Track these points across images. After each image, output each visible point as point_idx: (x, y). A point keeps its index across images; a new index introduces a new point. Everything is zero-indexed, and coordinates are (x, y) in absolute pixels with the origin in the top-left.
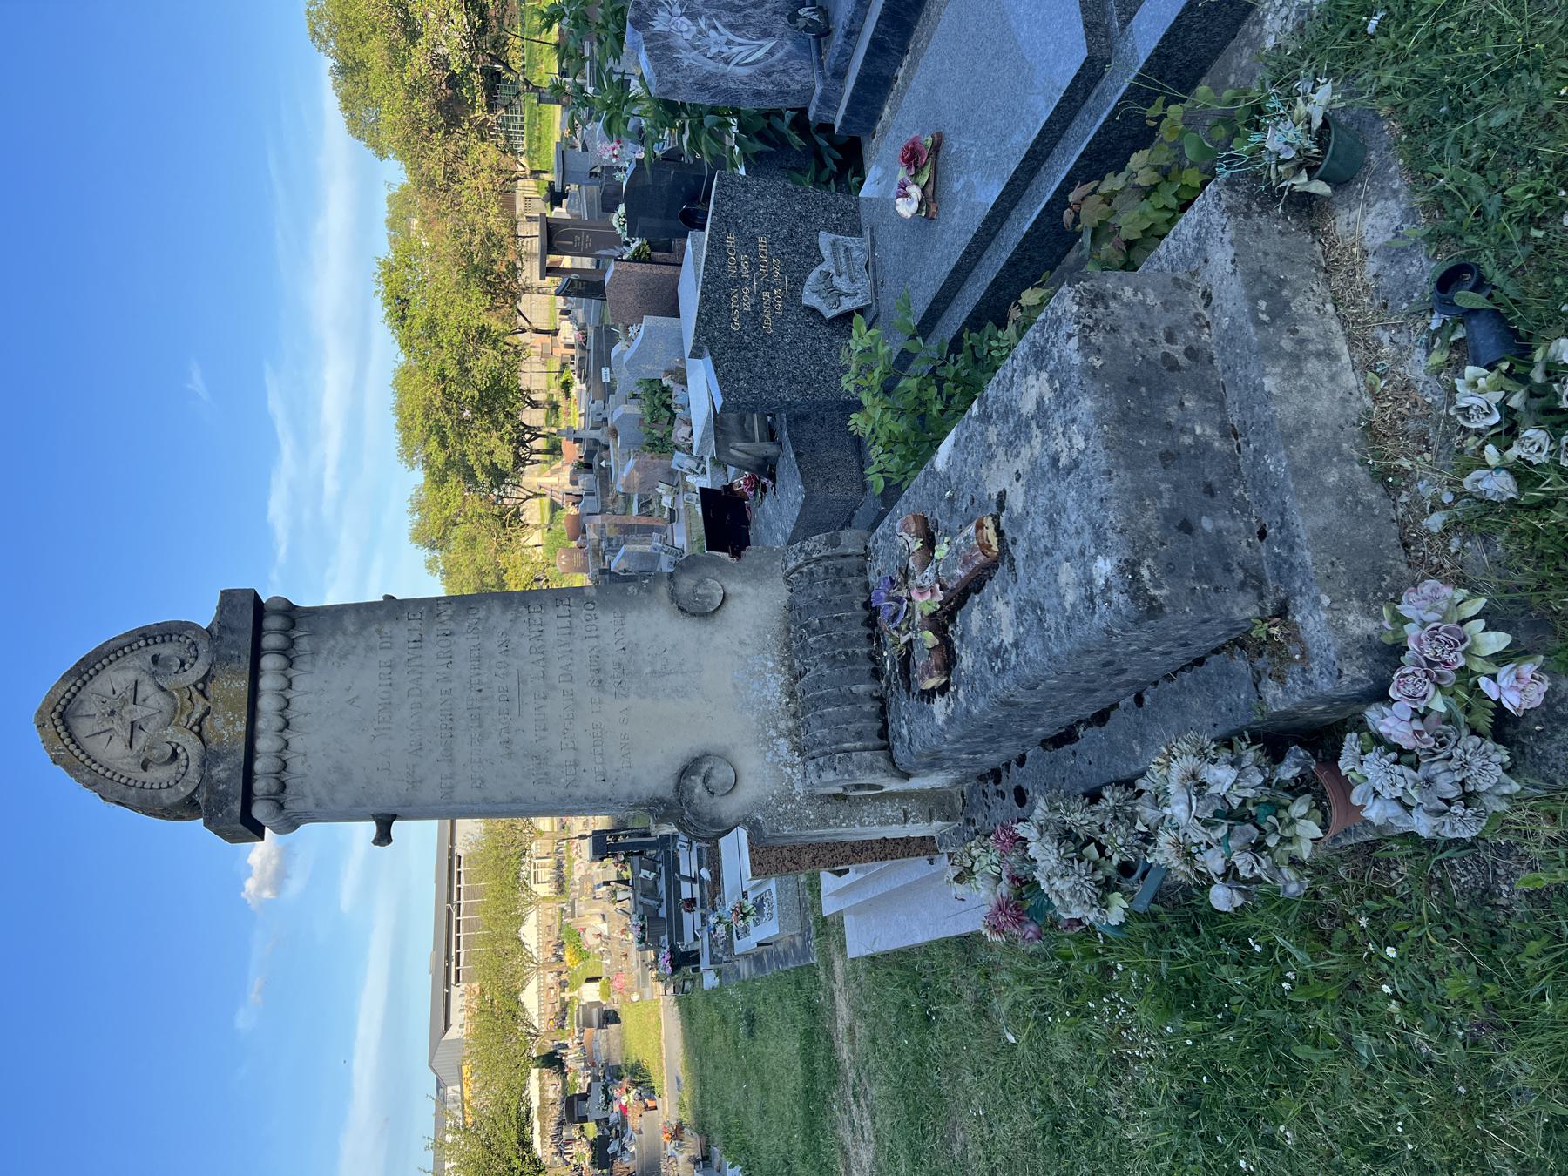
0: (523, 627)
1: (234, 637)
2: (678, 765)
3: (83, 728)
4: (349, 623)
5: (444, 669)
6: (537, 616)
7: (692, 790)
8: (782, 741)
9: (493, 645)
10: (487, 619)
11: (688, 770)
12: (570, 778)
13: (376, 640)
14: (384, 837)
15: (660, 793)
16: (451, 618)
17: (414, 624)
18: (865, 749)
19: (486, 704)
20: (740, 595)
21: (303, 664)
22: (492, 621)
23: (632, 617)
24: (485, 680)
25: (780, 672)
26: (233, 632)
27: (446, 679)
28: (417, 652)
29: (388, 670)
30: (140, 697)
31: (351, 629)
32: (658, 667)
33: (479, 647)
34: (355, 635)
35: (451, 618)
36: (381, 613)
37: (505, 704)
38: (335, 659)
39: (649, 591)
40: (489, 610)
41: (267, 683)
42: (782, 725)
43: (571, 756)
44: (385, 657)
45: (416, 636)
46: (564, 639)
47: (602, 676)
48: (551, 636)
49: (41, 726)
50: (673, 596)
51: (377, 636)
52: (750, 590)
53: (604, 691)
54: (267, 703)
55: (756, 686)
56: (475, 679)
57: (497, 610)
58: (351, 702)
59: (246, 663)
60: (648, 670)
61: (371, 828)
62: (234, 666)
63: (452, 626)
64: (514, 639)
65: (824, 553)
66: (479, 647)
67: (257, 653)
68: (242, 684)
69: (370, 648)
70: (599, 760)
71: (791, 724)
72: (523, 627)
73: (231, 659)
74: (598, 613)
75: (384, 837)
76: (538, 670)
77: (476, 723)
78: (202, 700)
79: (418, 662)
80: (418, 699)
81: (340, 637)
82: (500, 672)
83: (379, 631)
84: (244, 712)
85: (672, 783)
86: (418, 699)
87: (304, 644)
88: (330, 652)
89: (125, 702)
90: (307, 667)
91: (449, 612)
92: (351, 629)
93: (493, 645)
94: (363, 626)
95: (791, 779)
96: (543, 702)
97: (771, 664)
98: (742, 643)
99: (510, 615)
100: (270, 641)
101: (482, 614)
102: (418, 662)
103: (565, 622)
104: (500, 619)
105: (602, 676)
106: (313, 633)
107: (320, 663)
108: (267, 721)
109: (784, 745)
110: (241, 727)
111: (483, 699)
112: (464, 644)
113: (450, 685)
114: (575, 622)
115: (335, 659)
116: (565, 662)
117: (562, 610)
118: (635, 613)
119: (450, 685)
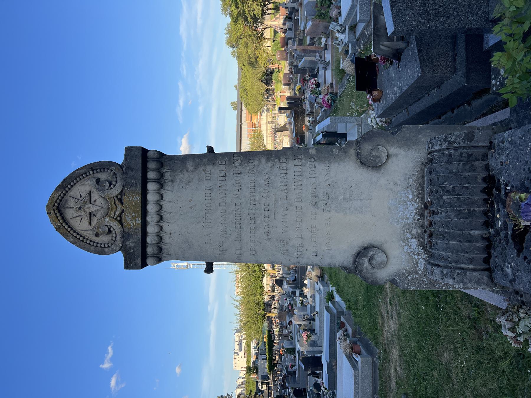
0: (276, 171)
1: (133, 173)
2: (355, 251)
3: (69, 214)
4: (190, 165)
5: (237, 193)
6: (284, 165)
7: (362, 265)
8: (414, 240)
9: (261, 180)
10: (258, 166)
11: (362, 252)
12: (299, 253)
13: (203, 175)
14: (209, 269)
15: (345, 264)
17: (222, 167)
18: (475, 270)
19: (258, 212)
20: (396, 155)
21: (168, 186)
22: (261, 166)
23: (335, 167)
24: (257, 199)
25: (416, 201)
26: (132, 170)
27: (238, 198)
28: (223, 183)
29: (210, 192)
30: (93, 200)
31: (191, 168)
32: (347, 196)
33: (254, 181)
34: (193, 172)
36: (205, 160)
37: (267, 213)
39: (345, 152)
40: (260, 161)
41: (151, 197)
42: (414, 231)
44: (208, 184)
45: (223, 174)
47: (317, 199)
49: (49, 213)
50: (358, 154)
51: (203, 173)
52: (402, 152)
53: (318, 208)
54: (151, 208)
55: (401, 209)
56: (252, 198)
57: (263, 161)
58: (192, 208)
59: (139, 187)
60: (342, 197)
61: (203, 265)
62: (134, 188)
63: (240, 169)
64: (272, 177)
65: (462, 144)
66: (254, 181)
67: (145, 181)
68: (138, 199)
69: (200, 179)
70: (314, 244)
71: (419, 231)
72: (276, 171)
73: (132, 185)
74: (316, 164)
75: (209, 269)
76: (284, 195)
77: (253, 222)
78: (120, 206)
79: (224, 188)
80: (225, 208)
82: (265, 195)
83: (204, 170)
84: (140, 213)
85: (351, 259)
86: (225, 208)
87: (168, 176)
89: (85, 202)
90: (169, 188)
91: (239, 161)
92: (191, 168)
93: (261, 180)
94: (197, 167)
95: (417, 262)
96: (286, 212)
97: (411, 197)
98: (395, 184)
99: (270, 164)
100: (151, 175)
101: (256, 163)
102: (224, 188)
103: (298, 169)
104: (265, 166)
105: (317, 199)
106: (172, 170)
107: (176, 187)
108: (152, 218)
109: (414, 243)
110: (139, 221)
111: (256, 209)
112: (246, 178)
114: (304, 168)
116: (298, 191)
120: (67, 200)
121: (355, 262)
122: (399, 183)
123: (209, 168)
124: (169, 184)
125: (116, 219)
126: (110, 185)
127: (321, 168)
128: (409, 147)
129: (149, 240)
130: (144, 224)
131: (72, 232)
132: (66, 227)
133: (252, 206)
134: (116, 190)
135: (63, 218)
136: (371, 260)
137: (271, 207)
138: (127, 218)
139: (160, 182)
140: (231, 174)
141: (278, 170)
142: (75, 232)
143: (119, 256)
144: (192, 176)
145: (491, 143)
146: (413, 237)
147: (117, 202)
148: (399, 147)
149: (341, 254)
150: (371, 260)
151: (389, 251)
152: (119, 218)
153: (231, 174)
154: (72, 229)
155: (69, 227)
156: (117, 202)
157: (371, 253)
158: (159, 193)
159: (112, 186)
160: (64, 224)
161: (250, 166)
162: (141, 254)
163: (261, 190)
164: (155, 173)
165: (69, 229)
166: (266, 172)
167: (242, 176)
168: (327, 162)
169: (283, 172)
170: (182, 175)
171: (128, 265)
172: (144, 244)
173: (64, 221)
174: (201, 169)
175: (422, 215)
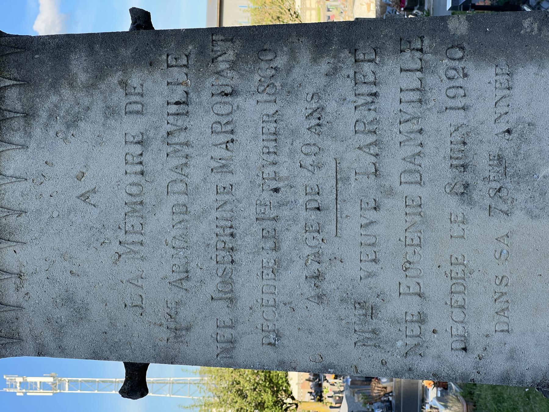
0: (344, 86)
4: (79, 66)
5: (221, 152)
6: (367, 68)
9: (296, 114)
10: (289, 71)
12: (411, 342)
13: (118, 97)
14: (135, 385)
16: (233, 65)
17: (178, 74)
19: (285, 212)
22: (297, 73)
23: (526, 76)
24: (284, 172)
27: (224, 168)
29: (138, 149)
31: (82, 77)
33: (276, 117)
34: (90, 87)
35: (233, 65)
36: (126, 52)
37: (313, 216)
38: (58, 126)
40: (293, 56)
43: (414, 306)
44: (133, 126)
45: (178, 94)
46: (411, 109)
47: (468, 177)
48: (389, 102)
51: (120, 91)
53: (471, 203)
56: (269, 171)
57: (305, 56)
58: (84, 197)
61: (117, 373)
63: (232, 79)
64: (331, 106)
66: (276, 117)
69: (110, 112)
70: (458, 315)
72: (344, 86)
74: (470, 66)
75: (135, 385)
76: (367, 161)
77: (270, 244)
79: (182, 138)
80: (183, 199)
81: (66, 92)
82: (308, 161)
83: (123, 84)
86: (183, 199)
88: (52, 116)
90: (17, 138)
91: (231, 55)
92: (82, 77)
93: (296, 114)
94: (100, 74)
96: (372, 215)
99: (324, 66)
101: (281, 61)
103: (411, 80)
104: (310, 72)
105: (468, 177)
106: (25, 83)
107: (37, 132)
111: (280, 205)
112: (251, 109)
113: (230, 179)
114: (431, 80)
115: (58, 126)
116: (410, 150)
117: (410, 59)
118: (532, 69)
119: (230, 179)
127: (483, 79)
133: (267, 196)
140: (205, 96)
141: (350, 83)
144: (86, 101)
153: (205, 96)
163: (298, 144)
166: (311, 90)
167: (238, 100)
168: (502, 60)
169: (364, 89)
170: (54, 99)
174: (114, 79)
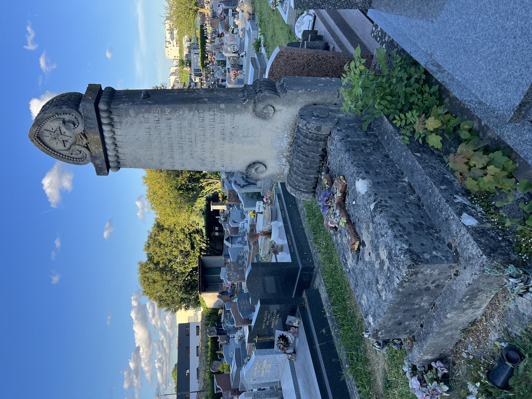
1: (91, 121)
2: (247, 164)
3: (47, 140)
6: (201, 114)
7: (251, 172)
8: (284, 159)
9: (185, 123)
11: (251, 165)
15: (241, 170)
16: (170, 113)
17: (156, 115)
18: (307, 192)
20: (280, 110)
21: (117, 126)
22: (185, 115)
23: (237, 117)
24: (183, 135)
25: (289, 138)
26: (90, 119)
28: (158, 125)
29: (148, 130)
30: (62, 132)
31: (133, 115)
32: (245, 134)
33: (181, 124)
34: (135, 117)
35: (170, 113)
37: (190, 143)
38: (128, 125)
39: (245, 107)
40: (184, 111)
41: (106, 134)
42: (285, 154)
43: (213, 159)
44: (147, 125)
45: (157, 119)
46: (212, 123)
47: (224, 136)
48: (207, 121)
49: (32, 141)
50: (254, 110)
52: (285, 108)
54: (108, 141)
55: (279, 142)
56: (180, 135)
58: (137, 139)
59: (97, 130)
60: (242, 135)
62: (94, 130)
63: (170, 116)
64: (193, 122)
65: (313, 132)
66: (181, 124)
67: (100, 124)
68: (98, 137)
70: (222, 161)
71: (288, 154)
73: (91, 128)
74: (225, 115)
78: (85, 139)
79: (159, 128)
81: (129, 118)
82: (188, 133)
83: (143, 117)
84: (101, 145)
85: (245, 168)
87: (116, 119)
88: (127, 123)
89: (58, 135)
91: (169, 111)
92: (133, 115)
93: (185, 123)
95: (284, 170)
96: (203, 143)
97: (286, 135)
98: (277, 128)
99: (192, 113)
100: (104, 121)
101: (181, 113)
102: (159, 128)
103: (212, 117)
105: (224, 136)
107: (124, 126)
108: (110, 147)
109: (284, 160)
110: (101, 150)
113: (170, 136)
114: (216, 117)
115: (128, 125)
116: (211, 131)
117: (211, 113)
118: (239, 115)
119: (170, 136)
120: (42, 132)
121: (247, 170)
122: (280, 127)
123: (146, 115)
124: (119, 124)
125: (84, 146)
126: (74, 125)
127: (228, 117)
128: (290, 106)
129: (109, 153)
130: (105, 150)
131: (53, 152)
132: (48, 149)
133: (179, 139)
134: (80, 129)
135: (44, 144)
136: (256, 170)
137: (193, 140)
138: (93, 148)
139: (111, 124)
140: (163, 120)
141: (198, 117)
142: (55, 151)
143: (90, 167)
144: (134, 120)
145: (330, 133)
146: (284, 157)
147: (82, 137)
148: (283, 105)
149: (239, 165)
150: (256, 170)
151: (267, 165)
152: (86, 146)
153: (163, 120)
154: (53, 150)
155: (50, 149)
156: (82, 137)
157: (257, 167)
158: (112, 131)
159: (76, 126)
160: (45, 147)
161: (177, 114)
162: (106, 165)
163: (186, 129)
164: (107, 119)
165: (50, 151)
166: (188, 119)
167: (172, 120)
168: (232, 114)
169: (201, 119)
170: (126, 119)
171: (99, 172)
172: (107, 162)
173: (45, 145)
174: (141, 115)
175: (291, 146)
